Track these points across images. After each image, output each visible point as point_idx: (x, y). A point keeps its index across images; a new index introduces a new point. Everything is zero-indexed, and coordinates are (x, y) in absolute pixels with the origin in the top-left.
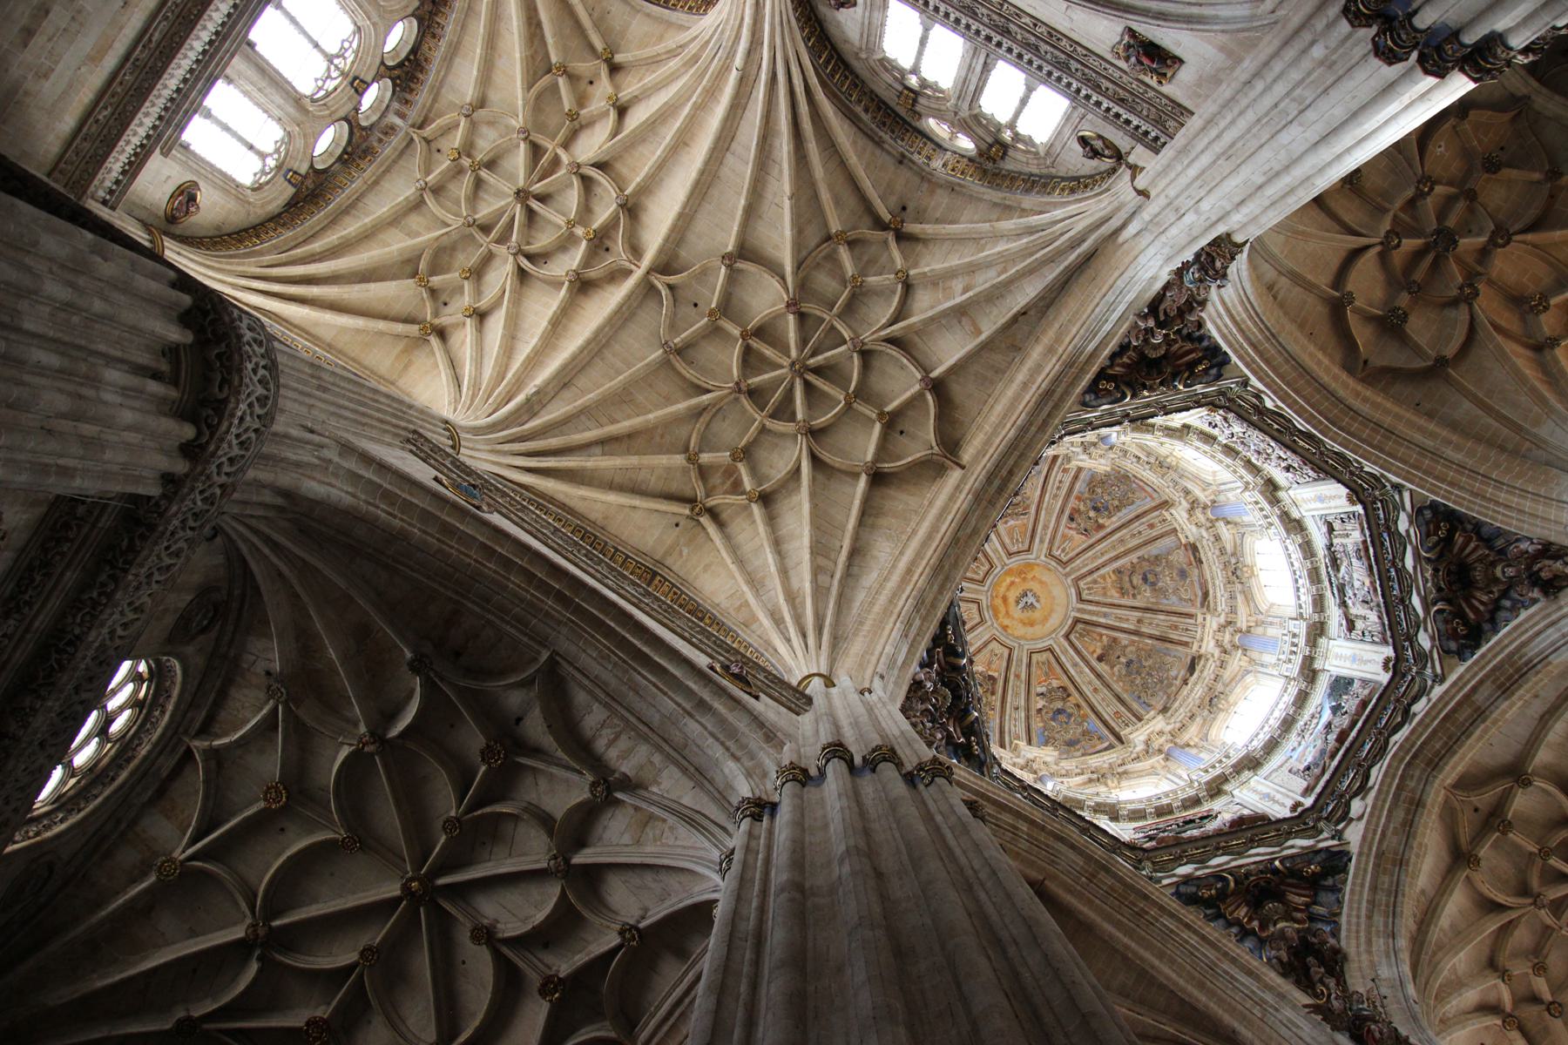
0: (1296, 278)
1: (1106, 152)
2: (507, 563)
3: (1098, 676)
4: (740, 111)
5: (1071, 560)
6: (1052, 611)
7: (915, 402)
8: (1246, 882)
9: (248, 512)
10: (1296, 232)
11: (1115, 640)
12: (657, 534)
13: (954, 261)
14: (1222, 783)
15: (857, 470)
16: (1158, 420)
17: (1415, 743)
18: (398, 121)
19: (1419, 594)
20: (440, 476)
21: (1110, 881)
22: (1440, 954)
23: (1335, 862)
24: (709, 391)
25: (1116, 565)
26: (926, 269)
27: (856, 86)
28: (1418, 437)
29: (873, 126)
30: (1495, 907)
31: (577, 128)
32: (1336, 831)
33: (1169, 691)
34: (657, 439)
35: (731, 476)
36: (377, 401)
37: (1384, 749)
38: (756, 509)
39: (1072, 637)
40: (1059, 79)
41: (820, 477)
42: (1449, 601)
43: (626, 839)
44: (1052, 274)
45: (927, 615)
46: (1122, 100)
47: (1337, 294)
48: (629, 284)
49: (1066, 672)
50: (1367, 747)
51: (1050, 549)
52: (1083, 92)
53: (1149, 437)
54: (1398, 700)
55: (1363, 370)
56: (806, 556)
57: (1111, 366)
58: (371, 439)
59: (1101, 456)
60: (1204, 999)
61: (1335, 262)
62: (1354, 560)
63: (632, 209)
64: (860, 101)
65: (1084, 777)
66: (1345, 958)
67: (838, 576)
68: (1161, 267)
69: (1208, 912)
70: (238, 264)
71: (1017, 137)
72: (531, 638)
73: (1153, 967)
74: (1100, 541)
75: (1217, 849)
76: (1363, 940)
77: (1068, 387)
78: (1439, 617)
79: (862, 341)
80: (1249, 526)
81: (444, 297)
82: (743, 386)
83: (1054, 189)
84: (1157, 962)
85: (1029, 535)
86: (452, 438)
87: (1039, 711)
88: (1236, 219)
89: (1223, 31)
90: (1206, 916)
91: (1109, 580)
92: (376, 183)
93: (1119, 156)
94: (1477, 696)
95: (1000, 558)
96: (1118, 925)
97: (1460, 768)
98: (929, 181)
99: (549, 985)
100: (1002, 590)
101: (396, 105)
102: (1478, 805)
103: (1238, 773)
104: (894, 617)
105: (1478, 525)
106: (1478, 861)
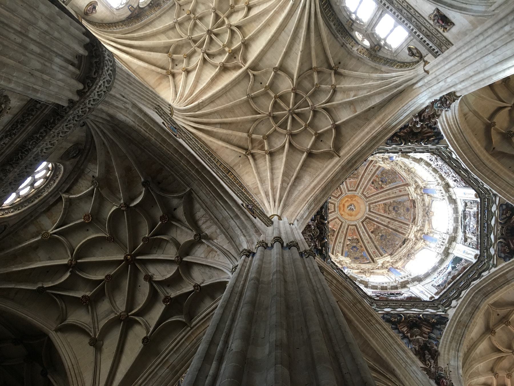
0: (476, 113)
1: (417, 55)
2: (181, 156)
3: (370, 238)
4: (290, 17)
5: (370, 197)
6: (359, 213)
7: (328, 131)
8: (408, 319)
9: (97, 120)
10: (480, 97)
11: (379, 227)
12: (233, 158)
13: (353, 85)
14: (406, 284)
15: (304, 150)
16: (411, 155)
17: (480, 286)
19: (494, 234)
20: (164, 122)
21: (360, 307)
22: (473, 362)
23: (442, 320)
24: (260, 114)
25: (384, 202)
26: (343, 86)
27: (333, 15)
28: (507, 179)
29: (336, 31)
31: (233, 12)
32: (445, 310)
33: (394, 248)
34: (239, 127)
35: (261, 144)
36: (147, 92)
37: (468, 286)
38: (267, 157)
39: (364, 223)
40: (407, 24)
41: (291, 151)
42: (504, 239)
43: (203, 256)
44: (386, 96)
45: (317, 204)
46: (428, 36)
47: (490, 122)
48: (240, 71)
49: (359, 234)
50: (463, 283)
51: (363, 192)
52: (414, 30)
53: (407, 160)
54: (477, 270)
55: (492, 151)
56: (281, 176)
57: (400, 132)
58: (144, 105)
59: (388, 163)
60: (385, 356)
61: (492, 110)
62: (472, 218)
63: (246, 45)
64: (333, 21)
65: (358, 271)
66: (439, 354)
67: (290, 184)
68: (427, 100)
69: (393, 326)
70: (107, 35)
71: (386, 44)
72: (184, 183)
73: (370, 340)
75: (401, 305)
76: (447, 349)
77: (383, 136)
78: (500, 244)
79: (315, 107)
80: (436, 198)
81: (176, 63)
82: (272, 115)
83: (394, 65)
84: (371, 339)
85: (357, 185)
86: (171, 111)
87: (348, 245)
88: (460, 87)
89: (473, 15)
90: (392, 327)
91: (381, 206)
92: (160, 17)
93: (421, 57)
94: (507, 275)
95: (345, 191)
96: (360, 323)
98: (351, 55)
99: (166, 299)
100: (344, 202)
102: (499, 313)
103: (413, 281)
104: (306, 202)
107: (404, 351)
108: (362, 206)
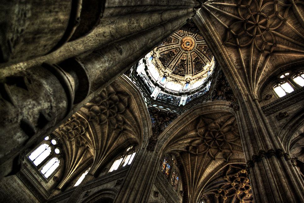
2: (94, 198)
5: (184, 33)
6: (191, 41)
7: (119, 97)
12: (123, 138)
18: (59, 138)
34: (111, 132)
42: (190, 27)
69: (217, 98)
78: (192, 30)
85: (176, 39)
95: (178, 46)
100: (183, 47)
101: (57, 138)
106: (239, 45)
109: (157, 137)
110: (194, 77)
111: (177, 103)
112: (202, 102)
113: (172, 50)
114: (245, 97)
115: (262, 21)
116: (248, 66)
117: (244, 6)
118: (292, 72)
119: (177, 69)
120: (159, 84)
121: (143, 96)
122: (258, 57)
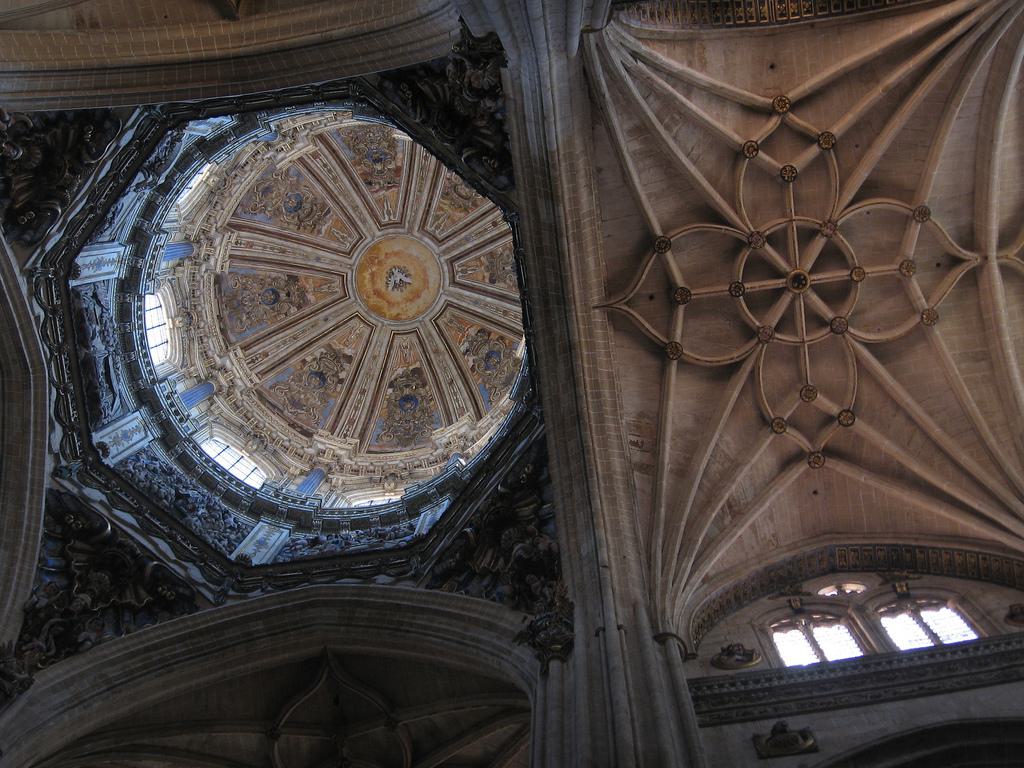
6: (424, 271)
11: (491, 254)
28: (307, 37)
30: (725, 373)
39: (457, 279)
42: (469, 144)
57: (14, 202)
74: (409, 181)
75: (465, 501)
78: (474, 164)
87: (473, 369)
91: (446, 207)
97: (593, 280)
100: (368, 286)
102: (650, 292)
105: (427, 68)
106: (676, 347)
107: (490, 626)
108: (414, 251)
109: (34, 669)
110: (363, 460)
111: (220, 541)
112: (368, 577)
113: (301, 273)
114: (620, 610)
115: (834, 275)
116: (683, 472)
117: (774, 162)
118: (881, 585)
119: (286, 384)
120: (164, 403)
121: (50, 411)
122: (748, 449)
